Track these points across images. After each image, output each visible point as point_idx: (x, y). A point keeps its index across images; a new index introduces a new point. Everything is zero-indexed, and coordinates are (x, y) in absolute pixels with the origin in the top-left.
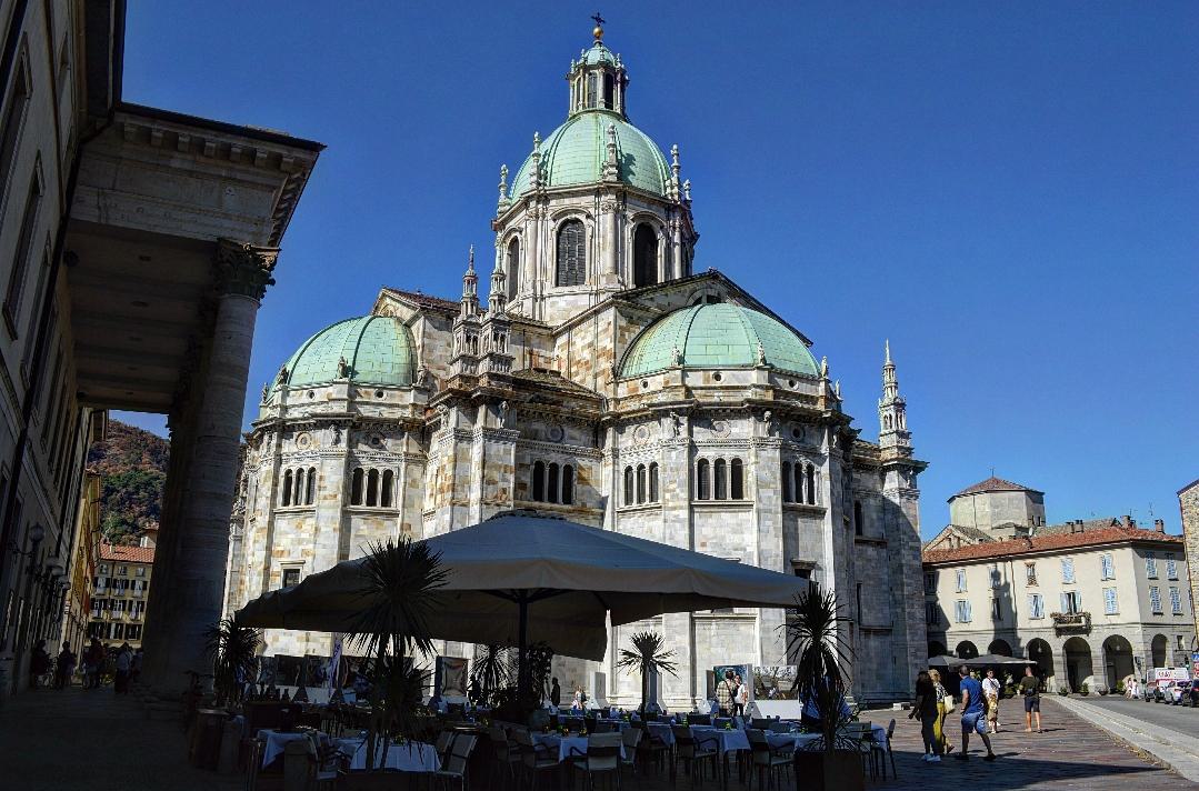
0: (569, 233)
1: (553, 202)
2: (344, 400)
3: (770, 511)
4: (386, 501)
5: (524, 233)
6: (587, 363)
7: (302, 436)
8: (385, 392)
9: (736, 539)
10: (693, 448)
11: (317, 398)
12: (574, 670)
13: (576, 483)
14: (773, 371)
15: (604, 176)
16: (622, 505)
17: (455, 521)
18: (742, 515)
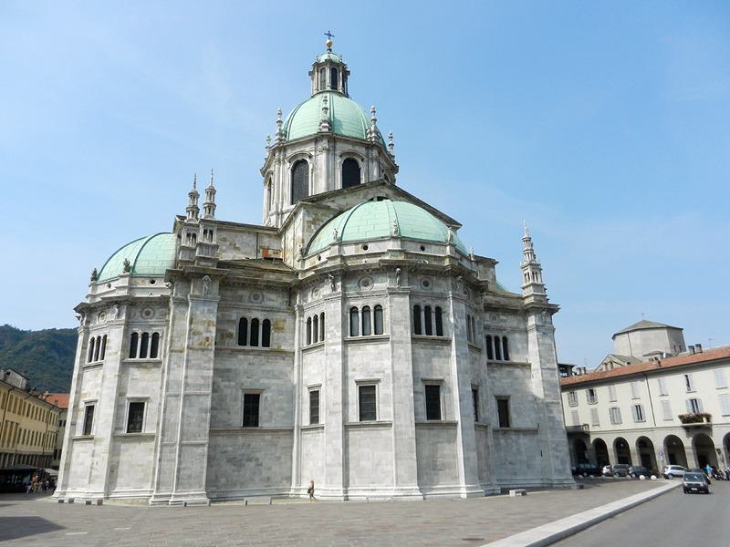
0: (299, 166)
1: (290, 153)
2: (124, 287)
3: (402, 342)
4: (154, 354)
9: (377, 365)
10: (345, 299)
11: (112, 288)
12: (270, 469)
13: (273, 332)
14: (403, 239)
16: (305, 345)
17: (172, 363)
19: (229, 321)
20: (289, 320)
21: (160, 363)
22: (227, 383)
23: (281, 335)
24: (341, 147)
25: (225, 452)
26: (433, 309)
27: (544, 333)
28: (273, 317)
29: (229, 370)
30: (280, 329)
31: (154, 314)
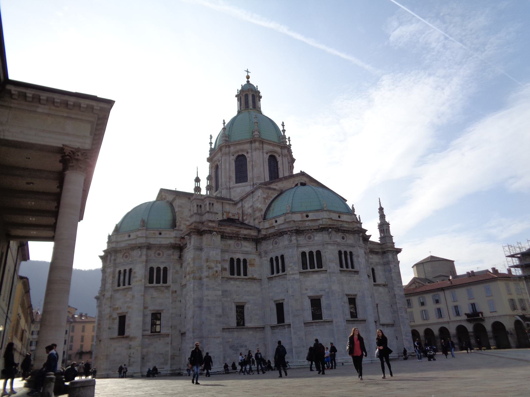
1: (232, 149)
4: (165, 281)
5: (220, 162)
6: (250, 214)
7: (125, 255)
8: (163, 233)
11: (131, 237)
14: (330, 211)
15: (253, 136)
18: (323, 275)
19: (224, 260)
20: (257, 259)
21: (169, 286)
22: (225, 299)
23: (253, 268)
24: (267, 148)
25: (228, 342)
26: (348, 253)
27: (395, 266)
28: (249, 258)
29: (226, 291)
30: (252, 265)
31: (163, 255)
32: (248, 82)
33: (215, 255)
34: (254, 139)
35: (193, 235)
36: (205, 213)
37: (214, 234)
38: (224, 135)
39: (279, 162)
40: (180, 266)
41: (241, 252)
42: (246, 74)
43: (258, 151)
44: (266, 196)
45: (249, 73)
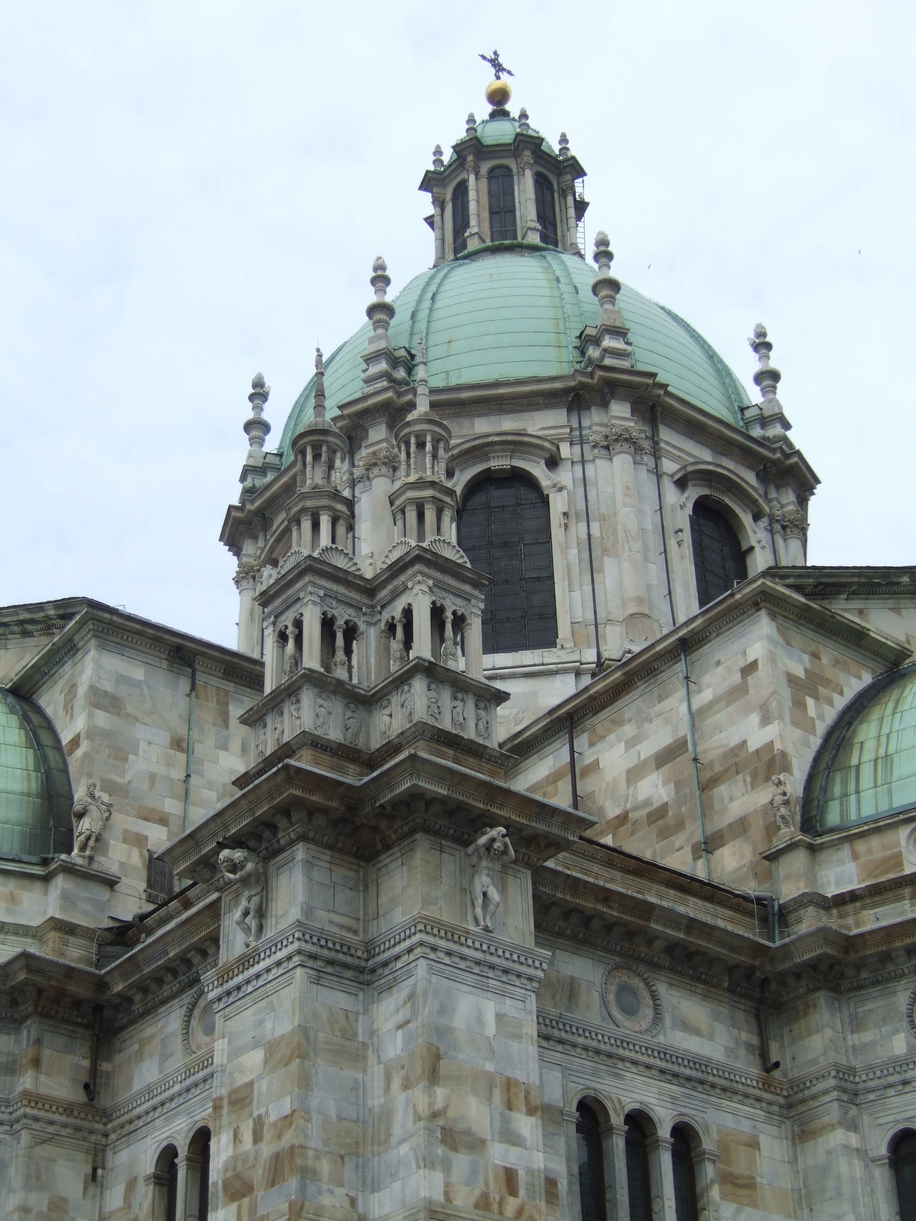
6: (661, 812)
13: (715, 1193)
32: (500, 114)
33: (491, 1028)
34: (599, 373)
35: (303, 838)
36: (402, 681)
37: (489, 847)
38: (382, 345)
39: (757, 550)
40: (89, 1169)
41: (658, 1062)
42: (487, 79)
43: (628, 458)
44: (806, 669)
45: (504, 76)
